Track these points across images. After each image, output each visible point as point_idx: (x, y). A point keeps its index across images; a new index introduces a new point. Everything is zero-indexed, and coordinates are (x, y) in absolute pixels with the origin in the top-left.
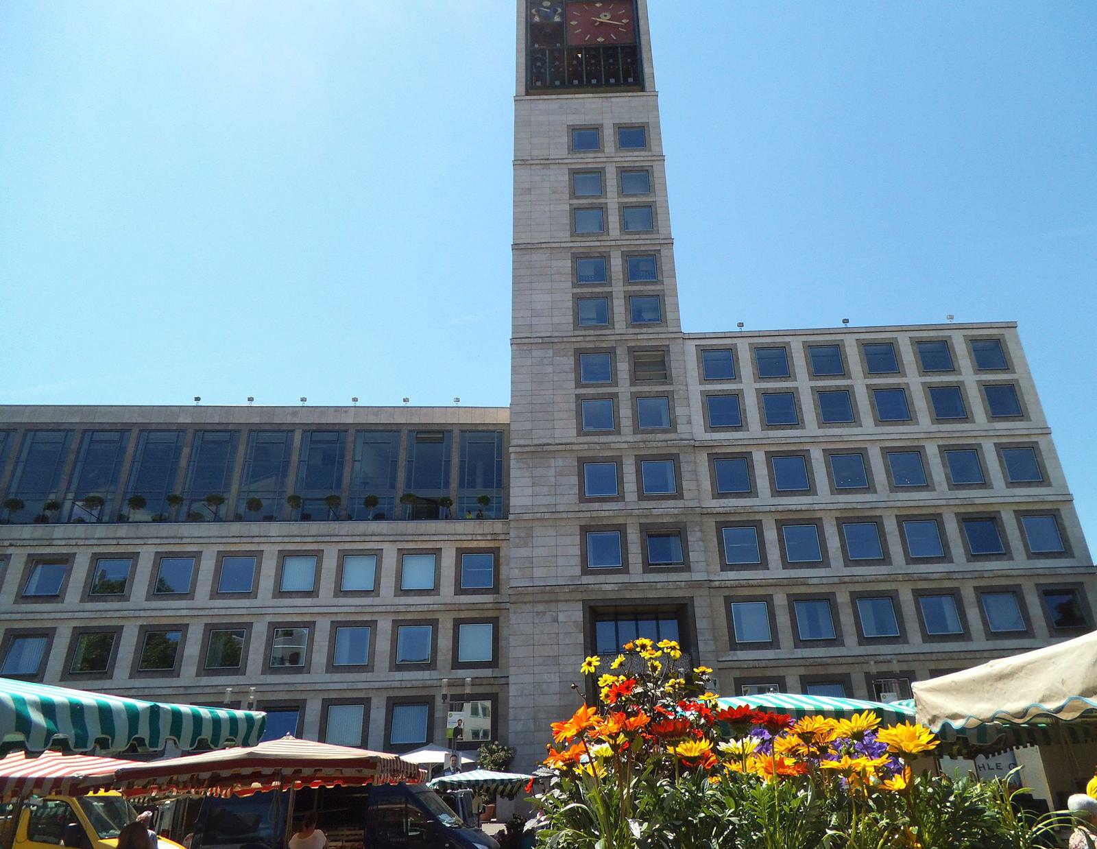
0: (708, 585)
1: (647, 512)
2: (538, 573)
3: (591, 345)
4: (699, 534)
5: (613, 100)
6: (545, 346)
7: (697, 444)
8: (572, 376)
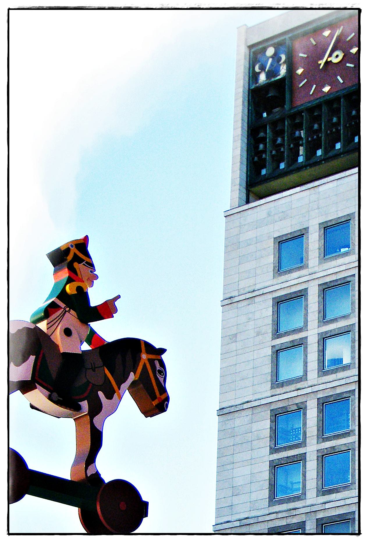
3: (284, 523)
5: (321, 188)
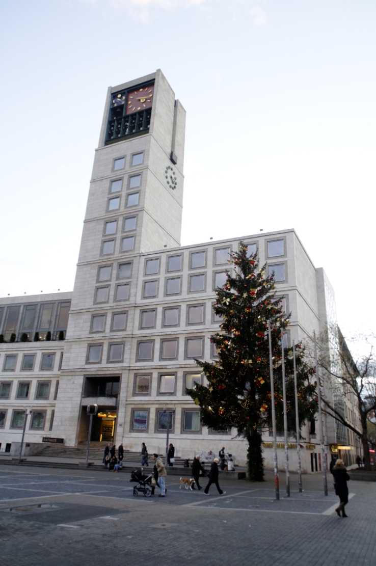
0: (130, 369)
1: (112, 337)
2: (71, 363)
3: (104, 263)
4: (129, 346)
6: (88, 265)
7: (137, 305)
8: (95, 278)
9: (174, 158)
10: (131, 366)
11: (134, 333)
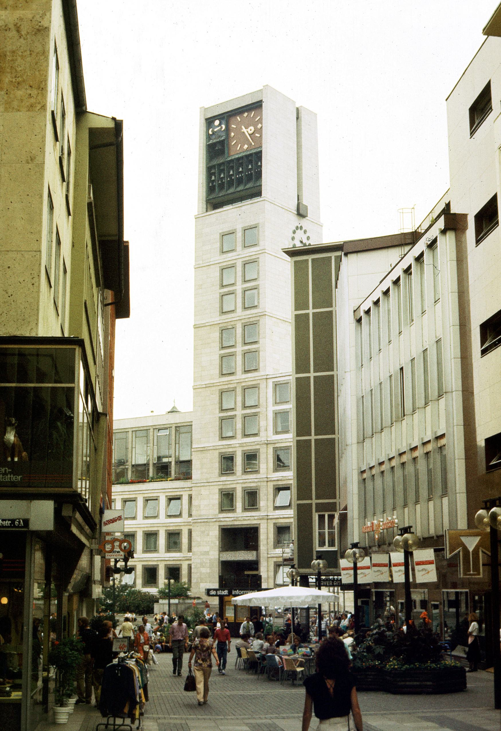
0: (267, 518)
1: (245, 481)
9: (301, 212)
10: (268, 514)
11: (268, 477)
